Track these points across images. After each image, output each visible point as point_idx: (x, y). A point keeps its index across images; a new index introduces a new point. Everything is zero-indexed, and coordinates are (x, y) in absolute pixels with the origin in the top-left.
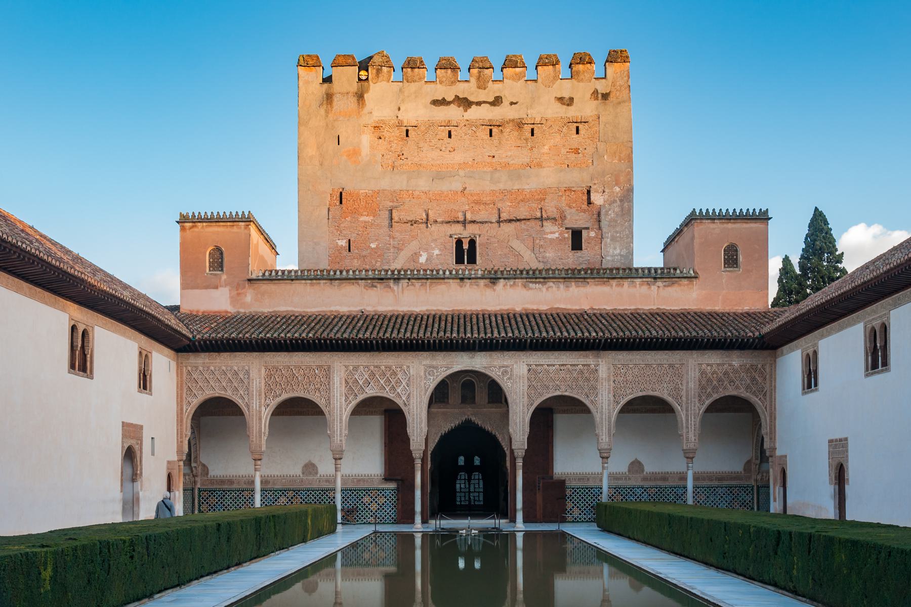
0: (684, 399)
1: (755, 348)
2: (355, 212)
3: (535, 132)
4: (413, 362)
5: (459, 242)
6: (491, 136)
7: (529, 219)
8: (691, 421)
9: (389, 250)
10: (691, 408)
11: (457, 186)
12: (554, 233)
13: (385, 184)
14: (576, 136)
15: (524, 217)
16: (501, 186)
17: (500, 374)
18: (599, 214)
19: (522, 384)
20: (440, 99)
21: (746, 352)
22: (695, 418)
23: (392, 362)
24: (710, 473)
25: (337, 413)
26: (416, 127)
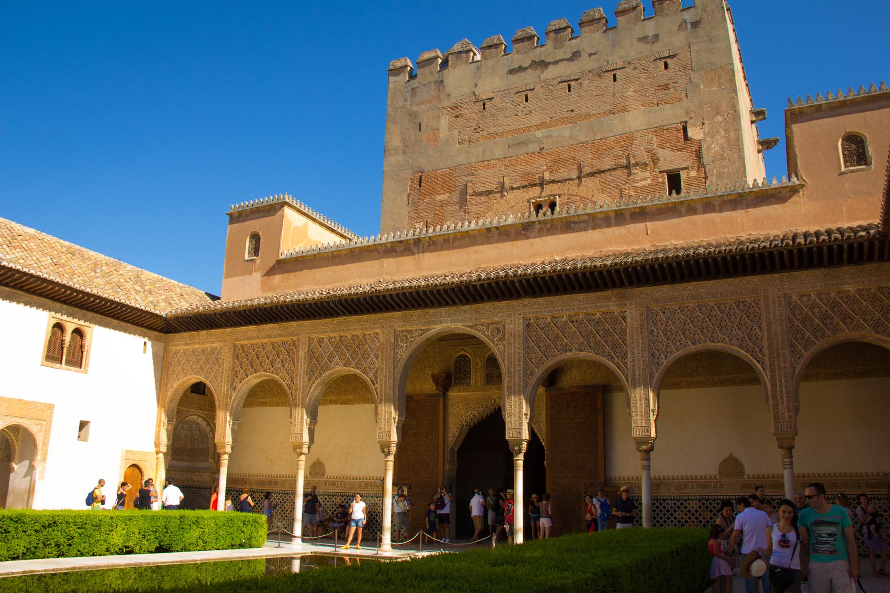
0: (766, 351)
3: (617, 77)
4: (383, 327)
6: (569, 90)
7: (616, 169)
10: (779, 365)
11: (534, 147)
12: (645, 179)
13: (461, 159)
14: (665, 72)
15: (609, 167)
17: (489, 334)
19: (517, 346)
20: (517, 67)
22: (786, 381)
23: (360, 329)
24: (856, 475)
25: (299, 395)
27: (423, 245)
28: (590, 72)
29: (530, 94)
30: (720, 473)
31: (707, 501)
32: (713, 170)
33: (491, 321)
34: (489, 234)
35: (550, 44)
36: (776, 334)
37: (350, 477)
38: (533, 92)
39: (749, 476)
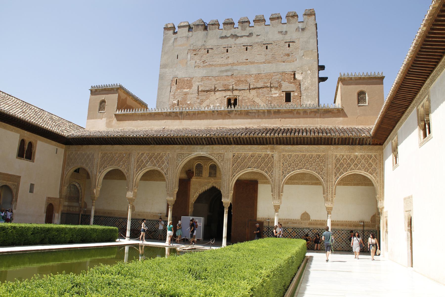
1: (369, 144)
2: (182, 88)
4: (171, 151)
5: (229, 100)
6: (247, 50)
7: (264, 88)
8: (330, 188)
9: (195, 104)
10: (330, 180)
11: (229, 73)
14: (288, 48)
16: (251, 73)
18: (300, 85)
20: (224, 36)
21: (364, 146)
22: (332, 186)
24: (350, 222)
26: (212, 49)
27: (184, 114)
28: (257, 43)
29: (229, 49)
30: (301, 219)
31: (295, 229)
32: (304, 93)
33: (218, 153)
34: (213, 113)
35: (240, 28)
36: (330, 169)
37: (146, 212)
38: (230, 48)
39: (312, 220)
